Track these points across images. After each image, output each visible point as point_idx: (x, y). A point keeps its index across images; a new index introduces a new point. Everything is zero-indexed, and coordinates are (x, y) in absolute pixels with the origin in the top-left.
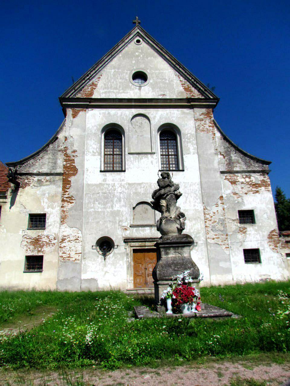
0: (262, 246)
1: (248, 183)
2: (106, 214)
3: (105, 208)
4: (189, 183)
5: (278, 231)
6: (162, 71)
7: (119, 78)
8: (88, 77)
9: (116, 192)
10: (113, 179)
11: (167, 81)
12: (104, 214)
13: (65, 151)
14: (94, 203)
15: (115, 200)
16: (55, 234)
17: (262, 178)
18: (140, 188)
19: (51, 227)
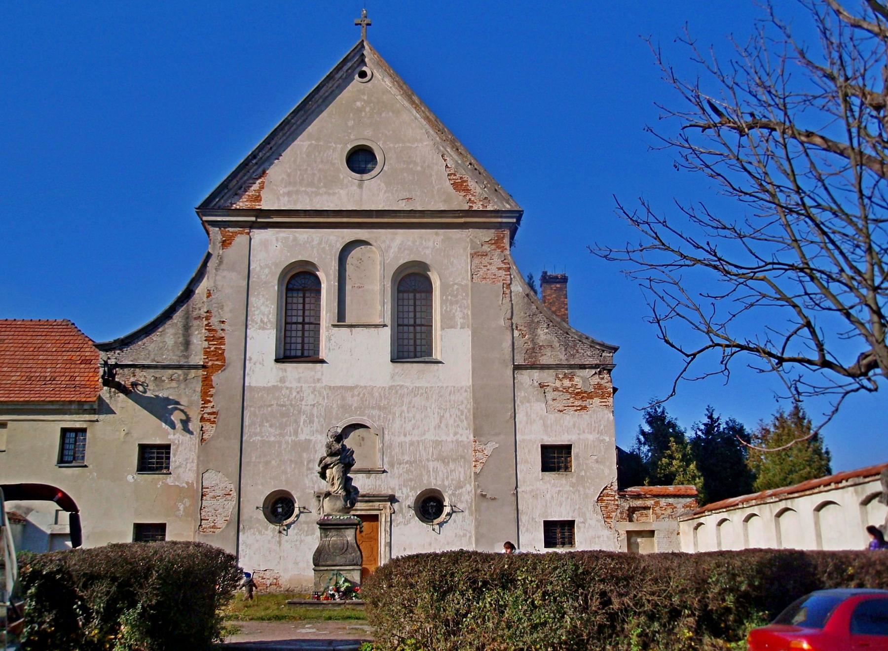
0: (583, 515)
1: (566, 390)
2: (284, 446)
3: (282, 435)
4: (449, 389)
5: (616, 487)
6: (409, 145)
7: (319, 160)
8: (254, 162)
9: (303, 403)
10: (300, 378)
11: (419, 168)
12: (280, 447)
13: (207, 318)
14: (261, 425)
15: (302, 421)
16: (187, 483)
17: (596, 380)
18: (352, 397)
19: (181, 470)
